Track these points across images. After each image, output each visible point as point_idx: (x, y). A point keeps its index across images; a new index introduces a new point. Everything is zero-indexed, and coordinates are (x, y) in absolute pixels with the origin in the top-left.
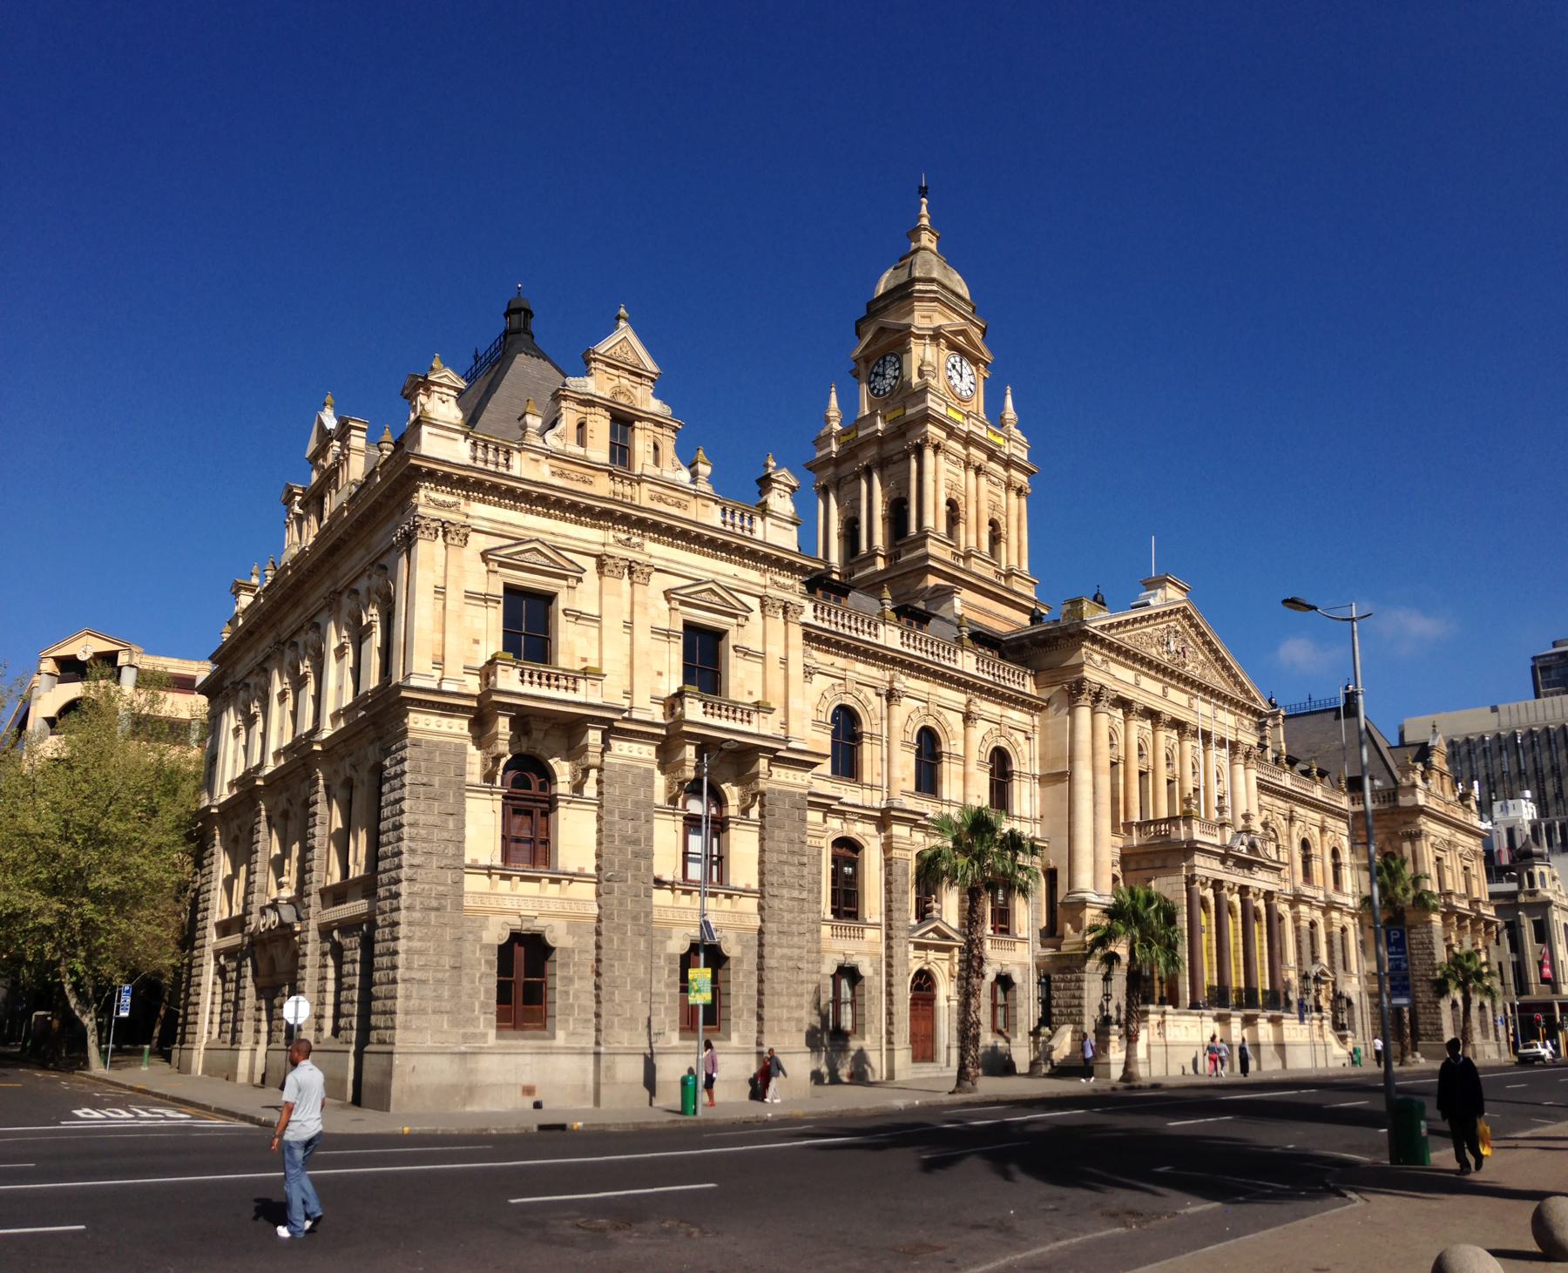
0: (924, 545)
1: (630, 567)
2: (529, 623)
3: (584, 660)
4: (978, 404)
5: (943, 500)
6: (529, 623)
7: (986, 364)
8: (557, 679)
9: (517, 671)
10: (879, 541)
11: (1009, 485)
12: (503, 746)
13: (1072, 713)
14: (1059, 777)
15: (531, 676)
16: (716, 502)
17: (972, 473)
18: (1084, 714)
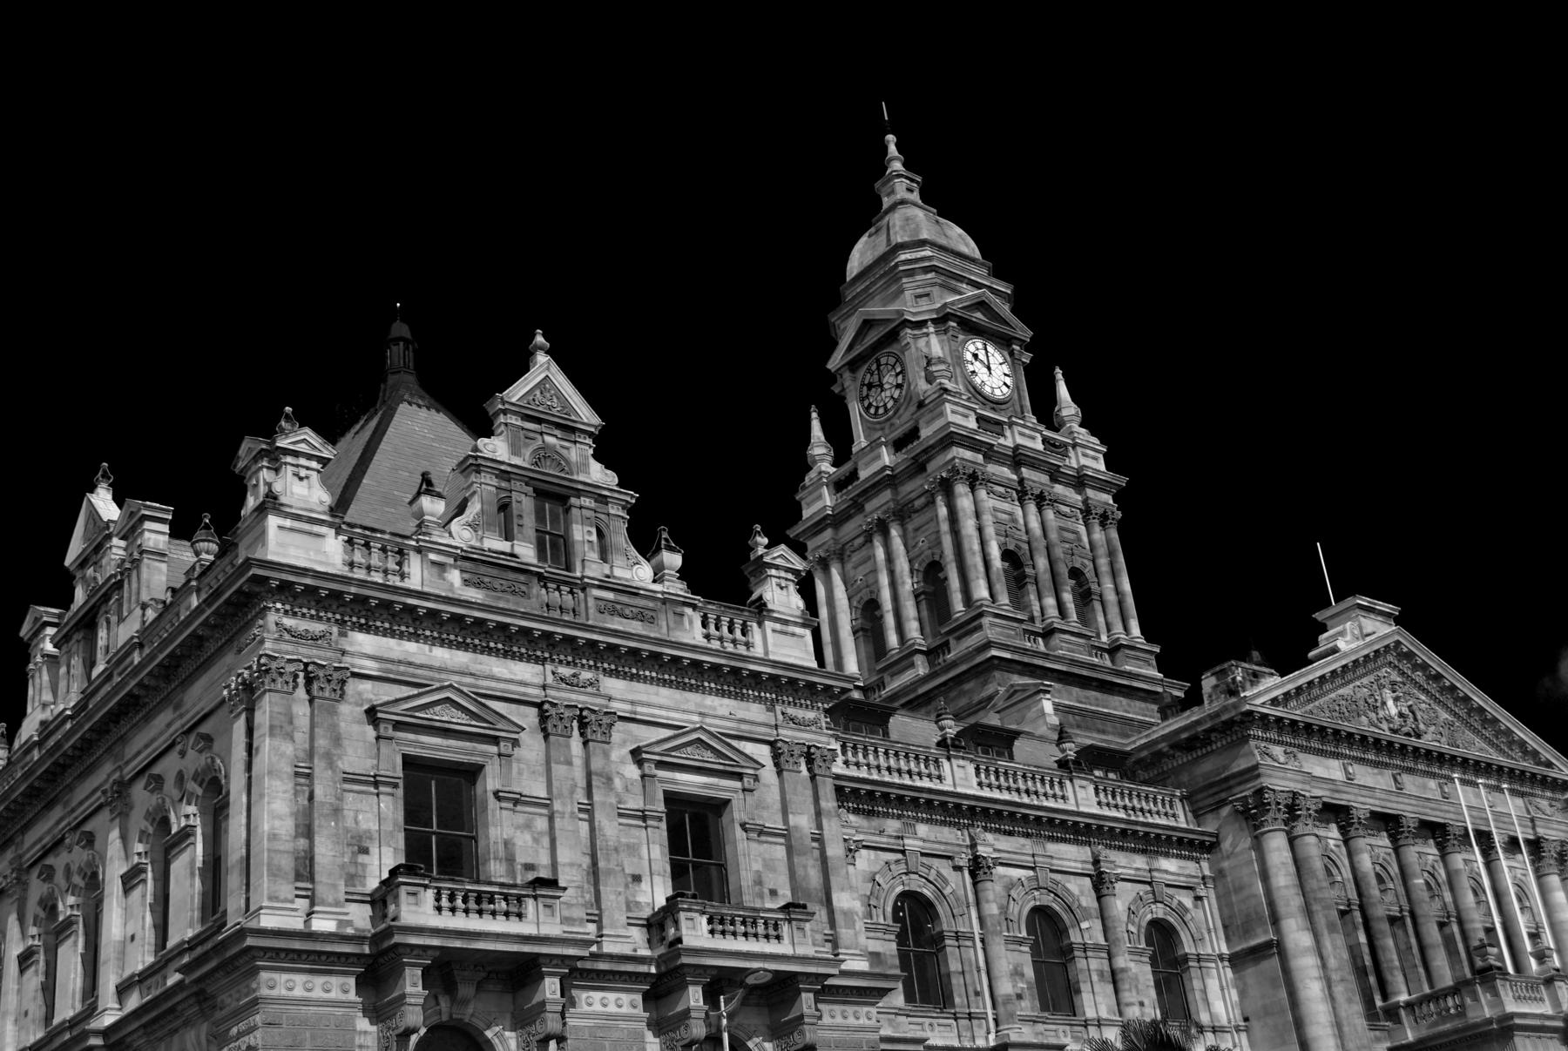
1: (581, 718)
2: (441, 817)
3: (529, 867)
5: (995, 552)
6: (441, 817)
8: (491, 901)
9: (430, 894)
12: (413, 1016)
13: (1258, 845)
14: (1258, 954)
15: (452, 898)
16: (694, 607)
17: (1032, 508)
18: (1277, 845)
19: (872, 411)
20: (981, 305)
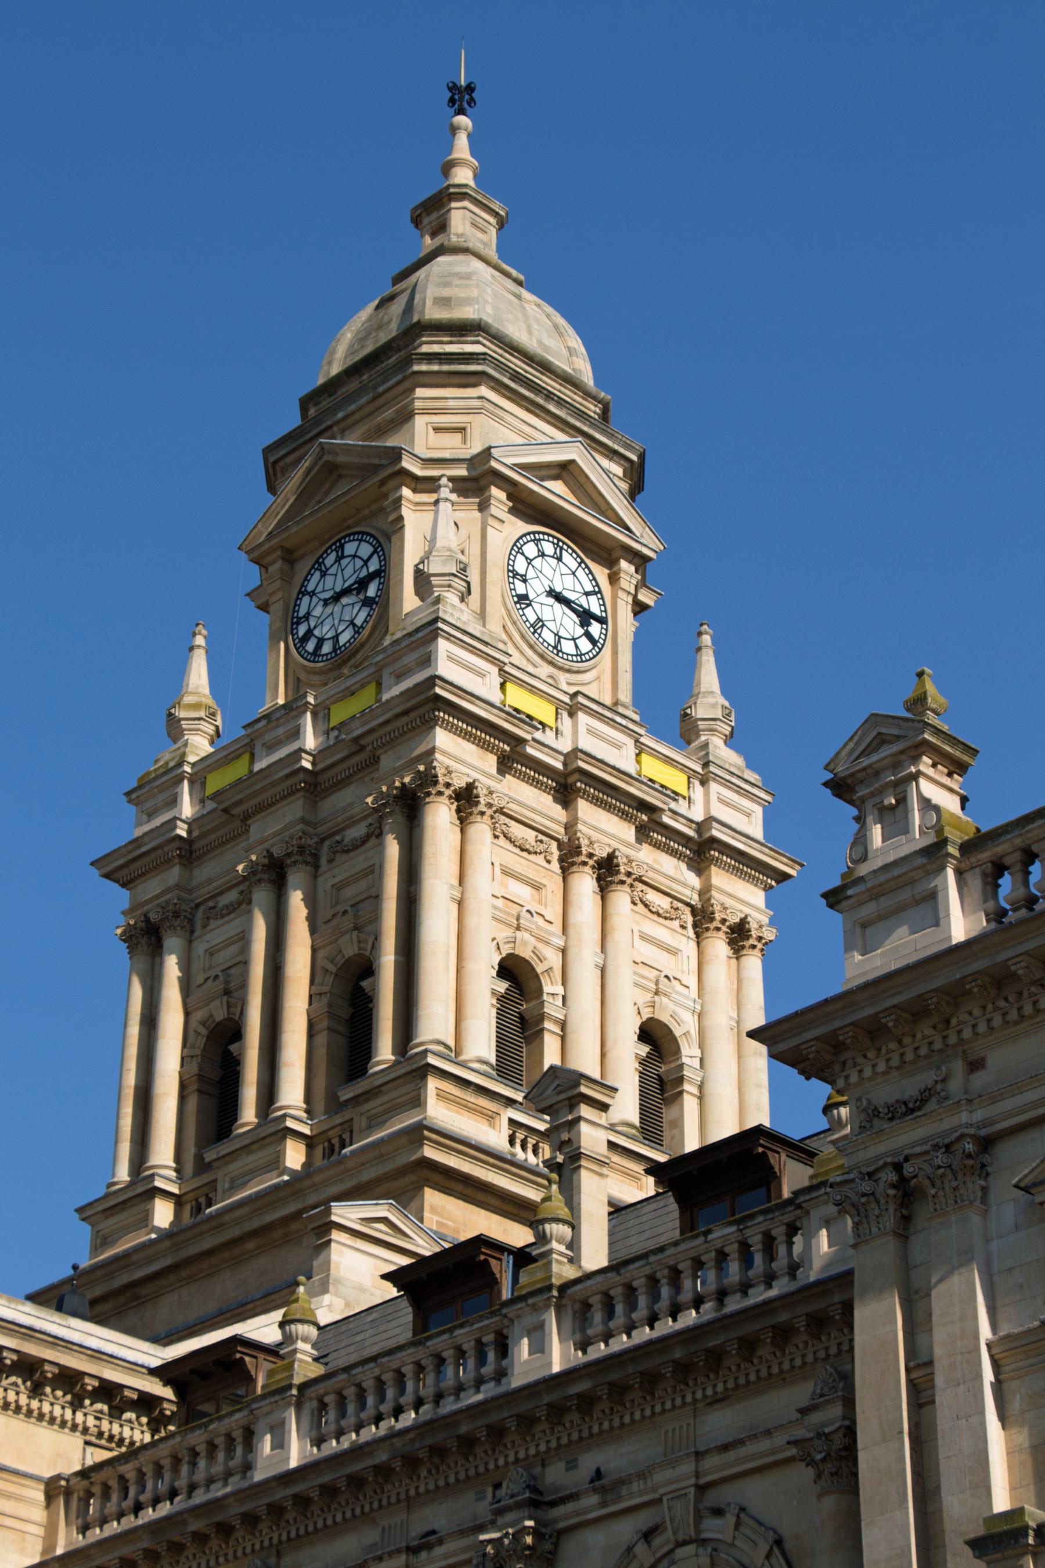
0: (418, 1102)
4: (610, 677)
7: (640, 561)
10: (292, 1092)
11: (702, 918)
17: (585, 883)
19: (310, 646)
20: (565, 470)
